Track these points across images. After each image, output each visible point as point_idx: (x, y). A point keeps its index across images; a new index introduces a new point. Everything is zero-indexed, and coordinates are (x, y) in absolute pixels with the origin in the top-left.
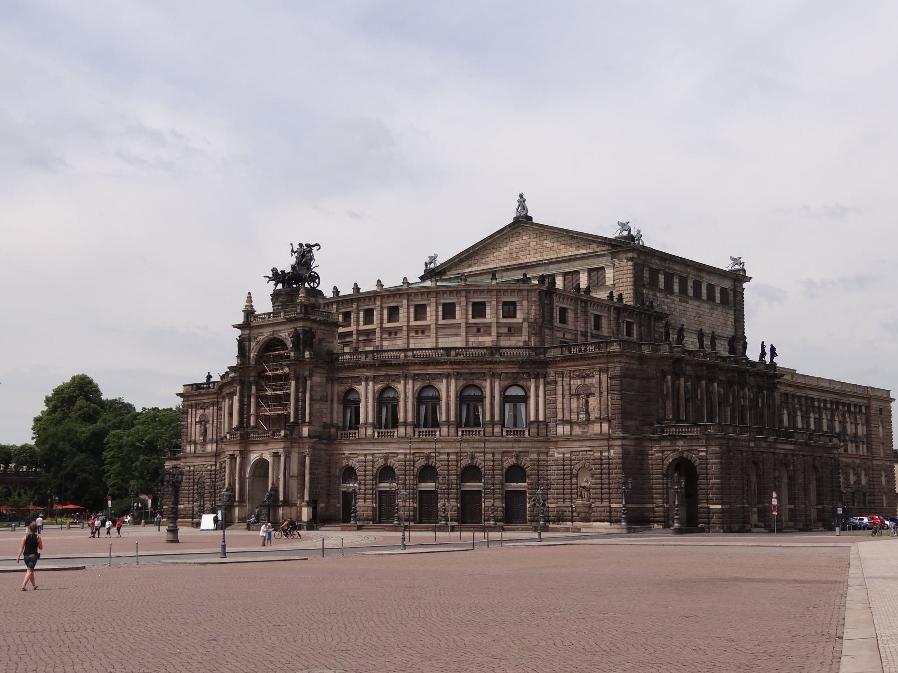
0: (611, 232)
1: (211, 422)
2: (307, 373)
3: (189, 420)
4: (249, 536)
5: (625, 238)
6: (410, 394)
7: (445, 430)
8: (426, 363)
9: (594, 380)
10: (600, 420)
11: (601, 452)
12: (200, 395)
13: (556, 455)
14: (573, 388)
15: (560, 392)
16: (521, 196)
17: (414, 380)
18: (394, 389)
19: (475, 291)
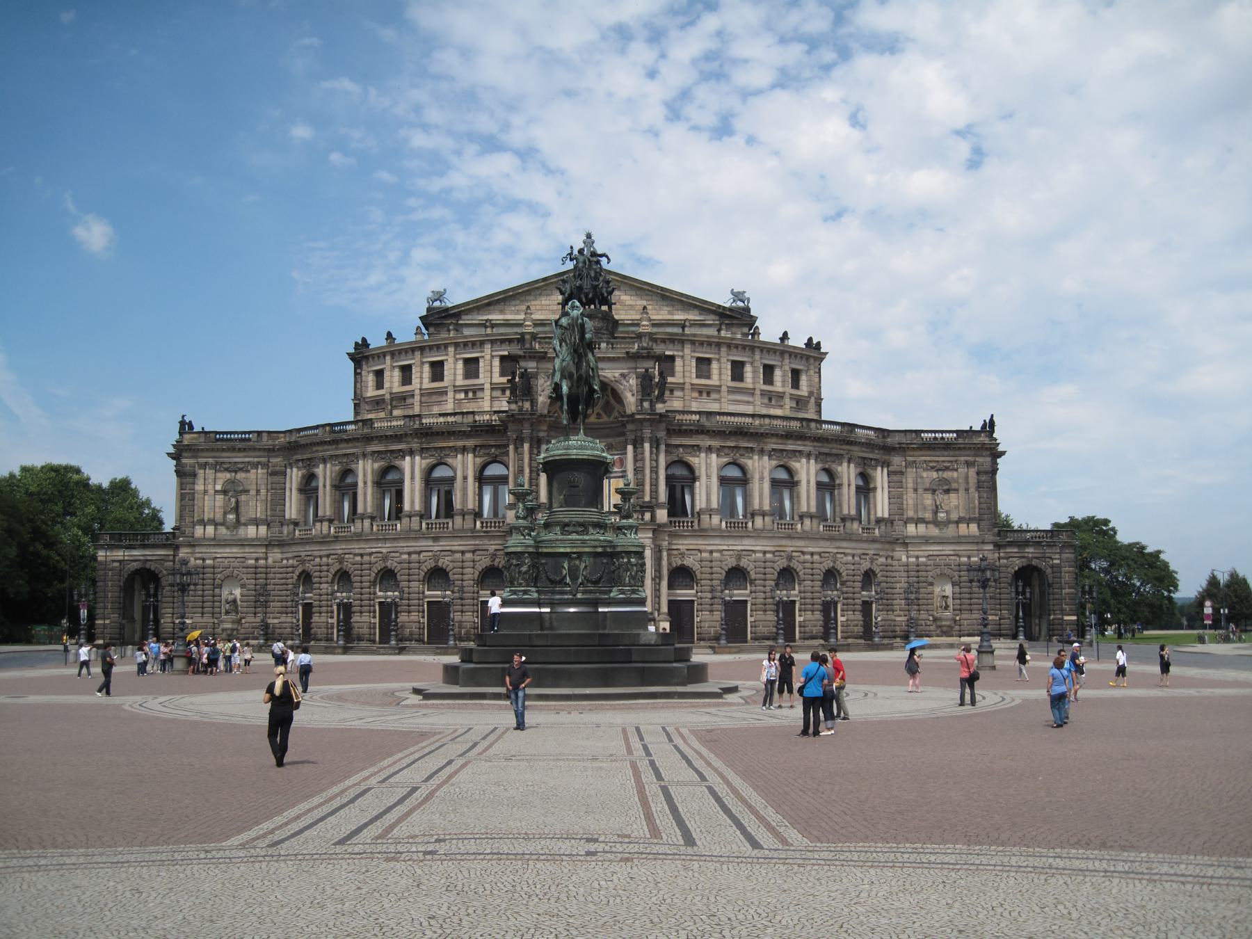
0: (725, 300)
1: (253, 492)
2: (662, 434)
3: (199, 487)
4: (740, 663)
5: (740, 308)
6: (766, 474)
7: (807, 522)
8: (789, 436)
9: (955, 474)
10: (968, 521)
11: (969, 557)
12: (233, 450)
13: (904, 559)
14: (927, 481)
15: (910, 485)
16: (589, 236)
17: (770, 456)
18: (742, 468)
19: (769, 350)
